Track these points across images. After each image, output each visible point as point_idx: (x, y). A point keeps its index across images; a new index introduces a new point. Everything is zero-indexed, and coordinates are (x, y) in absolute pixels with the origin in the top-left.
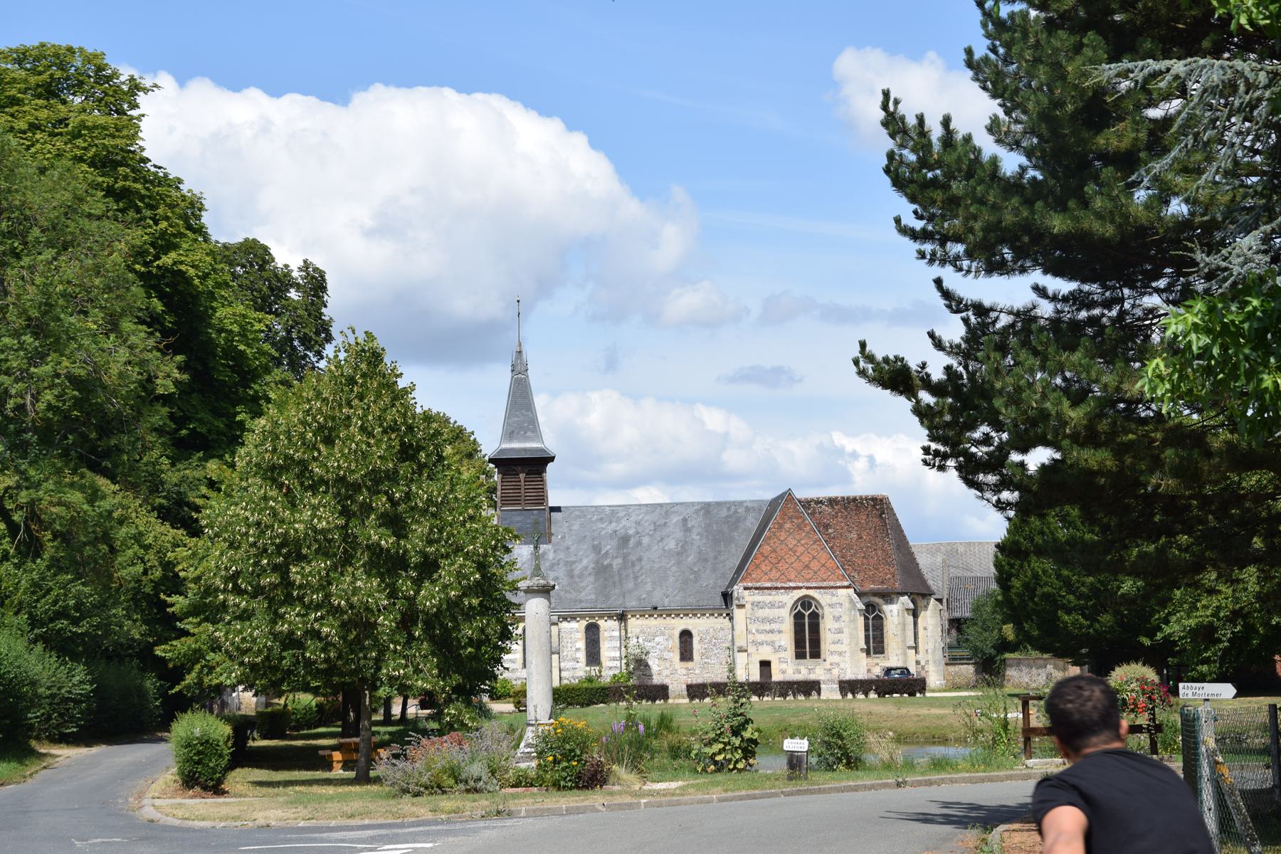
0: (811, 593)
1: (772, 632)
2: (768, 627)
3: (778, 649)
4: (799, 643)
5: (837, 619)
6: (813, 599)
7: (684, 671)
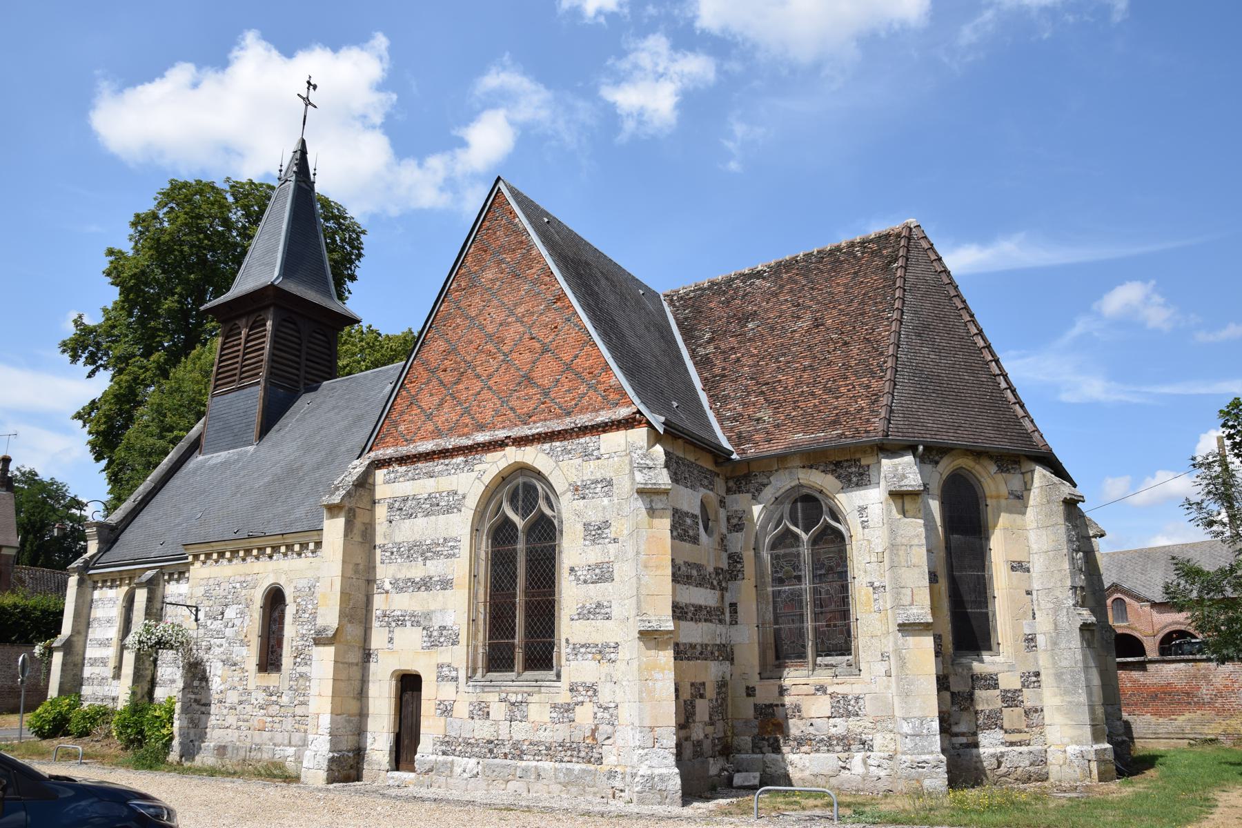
0: (532, 456)
1: (425, 584)
2: (417, 571)
3: (437, 638)
4: (499, 618)
5: (596, 532)
6: (539, 475)
7: (261, 697)
